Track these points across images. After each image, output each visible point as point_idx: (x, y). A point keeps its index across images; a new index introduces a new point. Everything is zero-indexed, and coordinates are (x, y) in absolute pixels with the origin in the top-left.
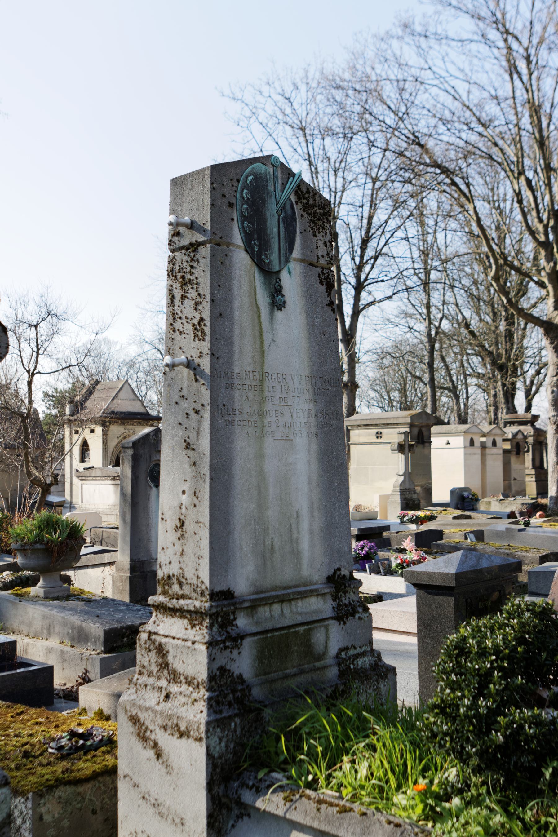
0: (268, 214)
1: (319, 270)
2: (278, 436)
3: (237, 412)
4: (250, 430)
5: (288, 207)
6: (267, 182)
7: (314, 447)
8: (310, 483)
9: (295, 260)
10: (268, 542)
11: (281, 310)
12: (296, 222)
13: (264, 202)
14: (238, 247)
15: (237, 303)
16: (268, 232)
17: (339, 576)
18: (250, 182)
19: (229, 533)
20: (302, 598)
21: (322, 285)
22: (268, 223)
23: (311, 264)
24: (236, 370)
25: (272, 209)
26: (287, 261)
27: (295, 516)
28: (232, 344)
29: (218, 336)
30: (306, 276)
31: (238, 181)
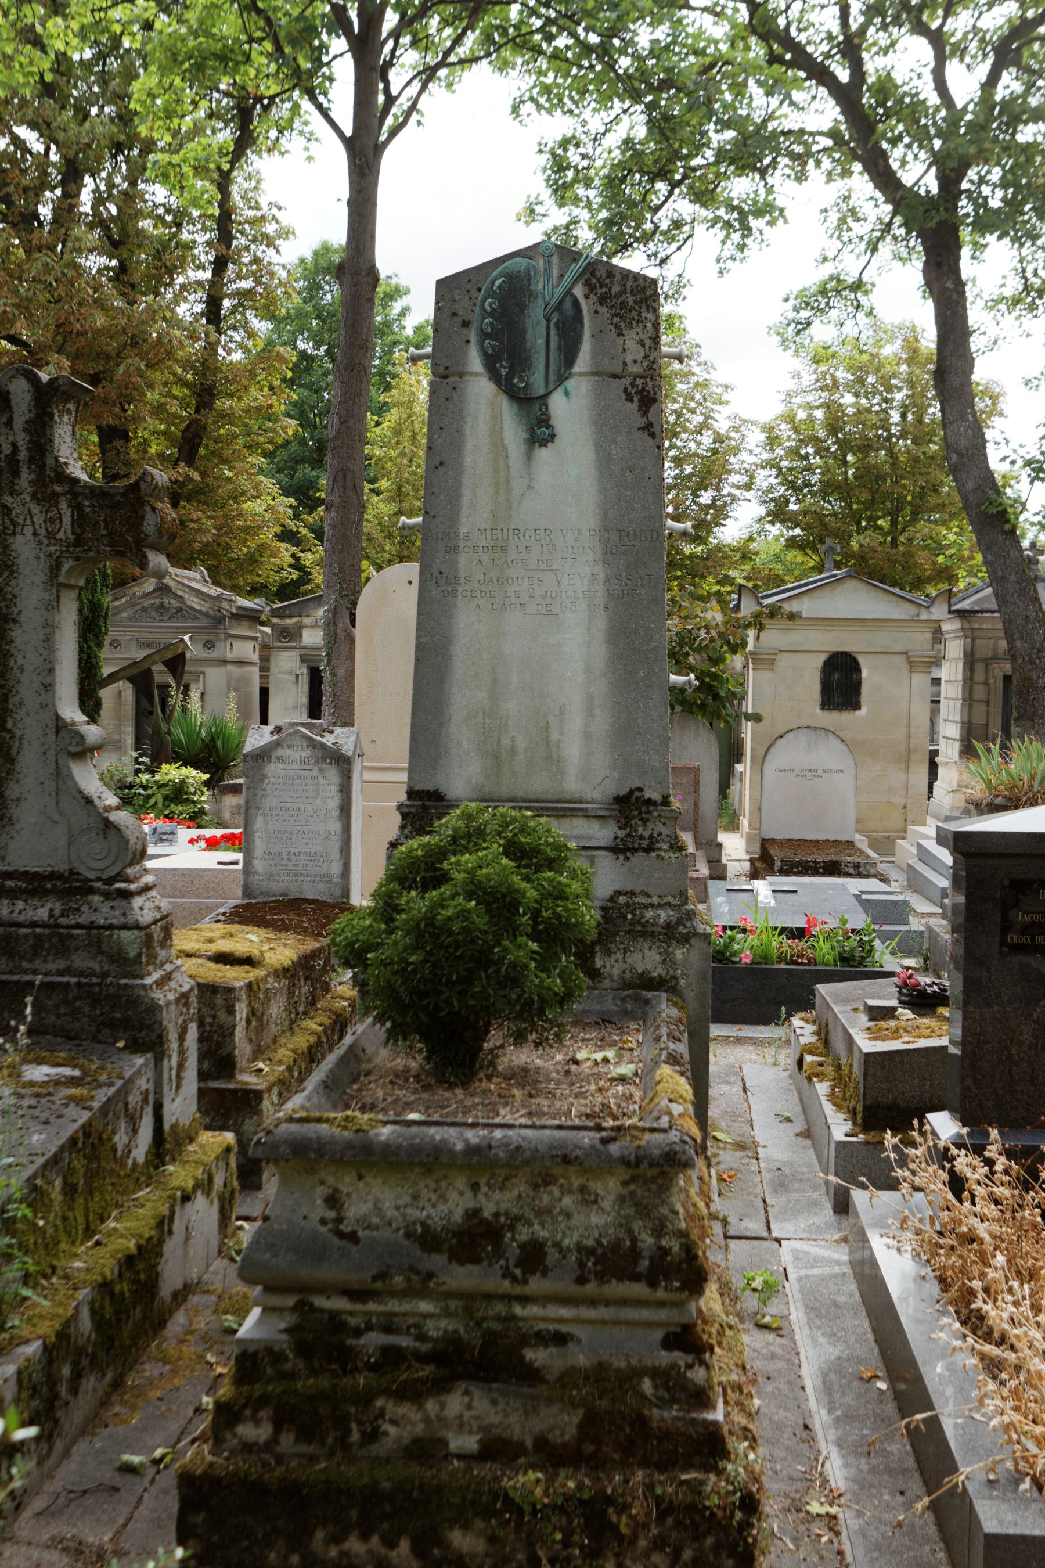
0: (529, 323)
1: (627, 381)
2: (532, 608)
3: (462, 581)
4: (482, 602)
5: (568, 305)
6: (529, 280)
7: (601, 623)
8: (588, 670)
9: (580, 374)
10: (506, 741)
11: (545, 446)
12: (582, 323)
13: (522, 308)
14: (477, 374)
15: (469, 446)
16: (528, 345)
17: (637, 798)
18: (500, 287)
19: (441, 725)
20: (558, 817)
21: (631, 400)
22: (529, 336)
23: (615, 376)
24: (463, 530)
25: (536, 315)
26: (561, 379)
27: (557, 712)
28: (459, 497)
29: (435, 490)
30: (598, 394)
31: (479, 290)
